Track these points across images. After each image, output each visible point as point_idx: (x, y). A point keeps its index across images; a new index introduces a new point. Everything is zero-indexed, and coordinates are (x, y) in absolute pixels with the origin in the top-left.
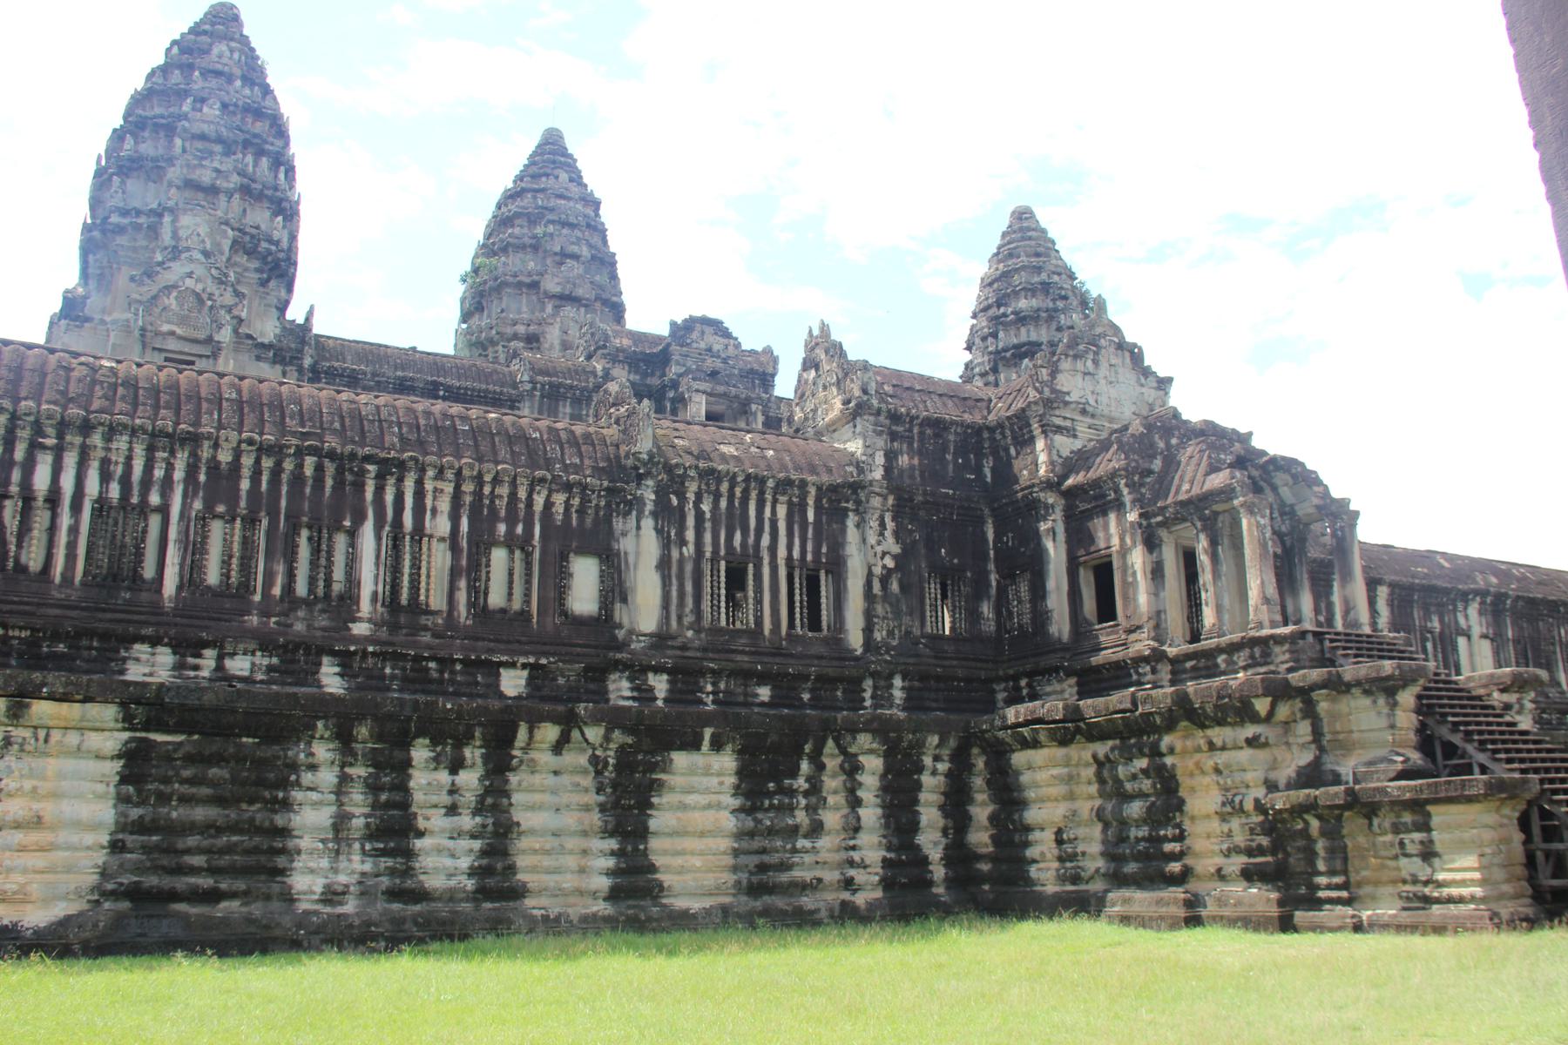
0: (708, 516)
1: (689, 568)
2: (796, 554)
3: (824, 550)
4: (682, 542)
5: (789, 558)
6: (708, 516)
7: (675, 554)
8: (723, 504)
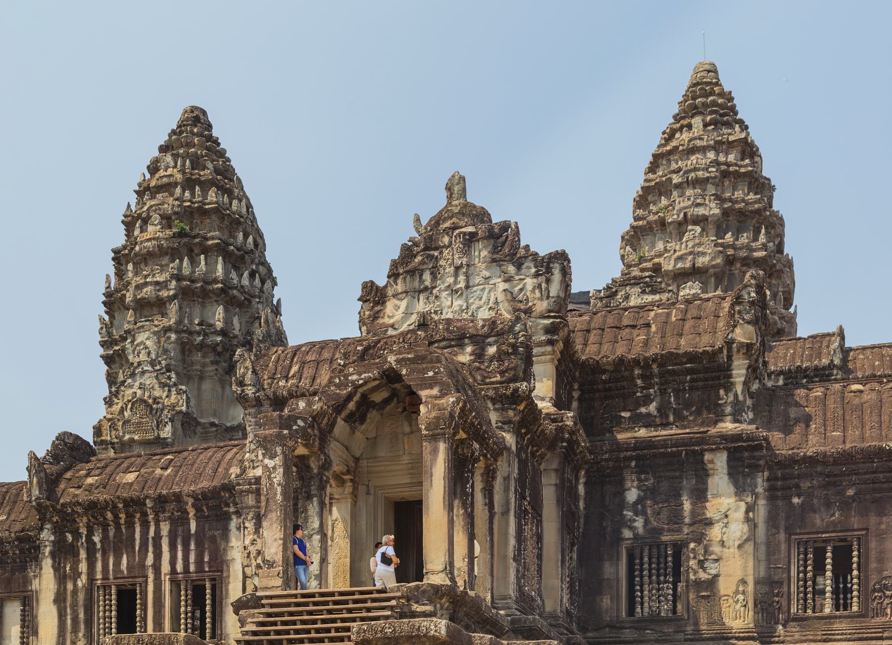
0: (99, 546)
1: (81, 596)
2: (179, 567)
3: (206, 559)
4: (76, 575)
5: (173, 571)
6: (99, 546)
7: (70, 586)
8: (111, 533)
